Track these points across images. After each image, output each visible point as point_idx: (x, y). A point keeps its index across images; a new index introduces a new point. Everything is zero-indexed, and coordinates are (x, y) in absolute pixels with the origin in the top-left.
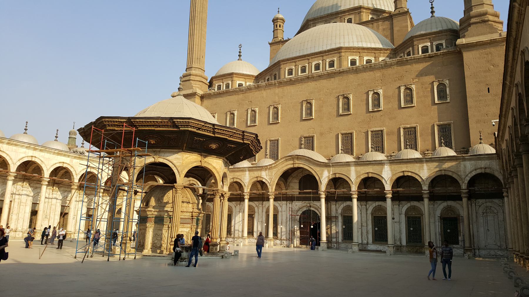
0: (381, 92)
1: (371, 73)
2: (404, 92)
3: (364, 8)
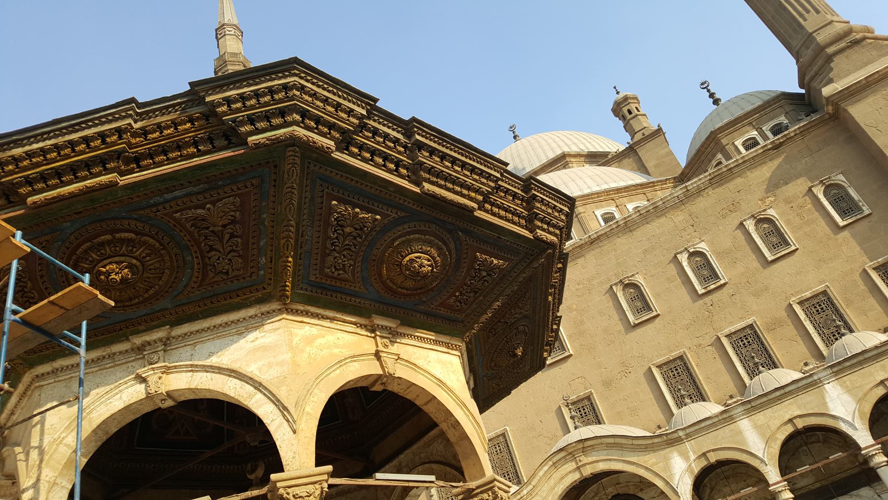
0: (703, 247)
1: (663, 220)
2: (757, 230)
3: (570, 155)
